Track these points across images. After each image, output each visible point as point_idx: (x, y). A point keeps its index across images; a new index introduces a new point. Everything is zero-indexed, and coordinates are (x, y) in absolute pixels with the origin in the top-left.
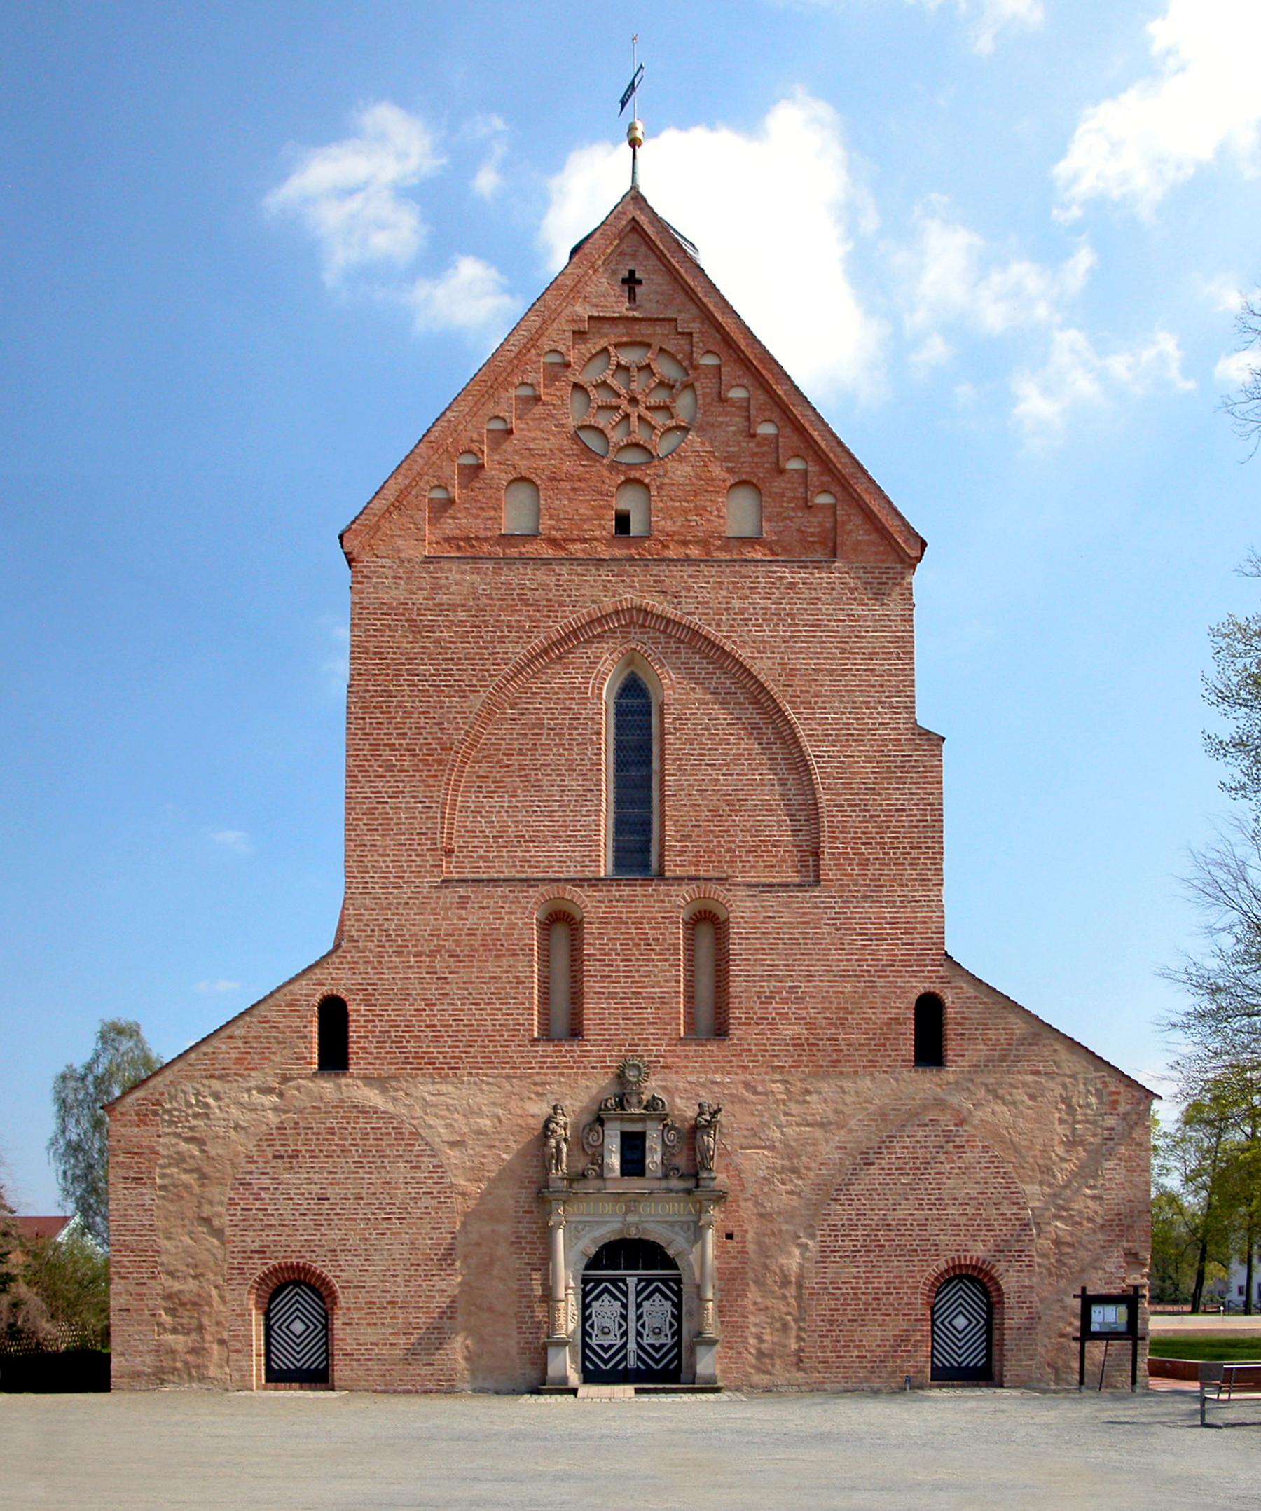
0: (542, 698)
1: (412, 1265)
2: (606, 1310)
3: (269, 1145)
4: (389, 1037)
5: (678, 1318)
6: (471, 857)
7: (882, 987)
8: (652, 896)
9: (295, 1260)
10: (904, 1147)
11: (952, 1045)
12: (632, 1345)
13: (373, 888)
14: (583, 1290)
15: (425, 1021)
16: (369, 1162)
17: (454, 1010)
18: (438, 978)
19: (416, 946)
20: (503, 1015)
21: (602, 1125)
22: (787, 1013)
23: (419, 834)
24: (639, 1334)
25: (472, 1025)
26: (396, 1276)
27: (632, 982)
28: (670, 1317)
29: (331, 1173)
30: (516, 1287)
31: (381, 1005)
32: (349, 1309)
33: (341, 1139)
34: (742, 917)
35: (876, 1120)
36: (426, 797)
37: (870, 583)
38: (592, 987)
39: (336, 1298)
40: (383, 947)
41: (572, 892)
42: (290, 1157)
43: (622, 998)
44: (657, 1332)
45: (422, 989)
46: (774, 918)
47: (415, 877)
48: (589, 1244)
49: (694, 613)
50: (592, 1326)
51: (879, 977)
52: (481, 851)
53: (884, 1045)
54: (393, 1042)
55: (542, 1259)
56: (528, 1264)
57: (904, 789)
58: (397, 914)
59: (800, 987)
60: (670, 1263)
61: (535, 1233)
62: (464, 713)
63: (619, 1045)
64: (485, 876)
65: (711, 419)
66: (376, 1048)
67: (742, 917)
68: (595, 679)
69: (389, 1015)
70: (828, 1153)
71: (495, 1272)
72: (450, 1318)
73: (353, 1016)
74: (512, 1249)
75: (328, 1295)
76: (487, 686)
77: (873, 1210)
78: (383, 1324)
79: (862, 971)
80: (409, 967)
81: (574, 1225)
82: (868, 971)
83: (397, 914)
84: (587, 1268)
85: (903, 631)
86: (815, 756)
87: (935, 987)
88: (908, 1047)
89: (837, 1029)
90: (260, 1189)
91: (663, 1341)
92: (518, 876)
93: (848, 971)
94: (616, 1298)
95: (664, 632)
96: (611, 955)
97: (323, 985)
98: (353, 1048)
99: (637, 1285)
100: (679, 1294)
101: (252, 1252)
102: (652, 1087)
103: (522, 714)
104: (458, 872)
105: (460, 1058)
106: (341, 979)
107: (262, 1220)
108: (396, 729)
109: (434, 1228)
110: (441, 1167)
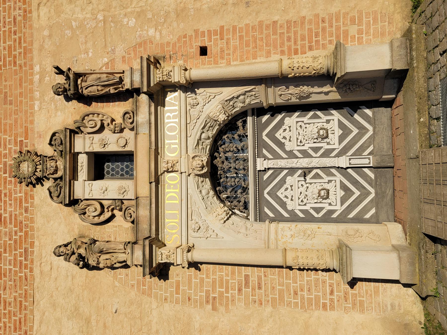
63: (5, 183)
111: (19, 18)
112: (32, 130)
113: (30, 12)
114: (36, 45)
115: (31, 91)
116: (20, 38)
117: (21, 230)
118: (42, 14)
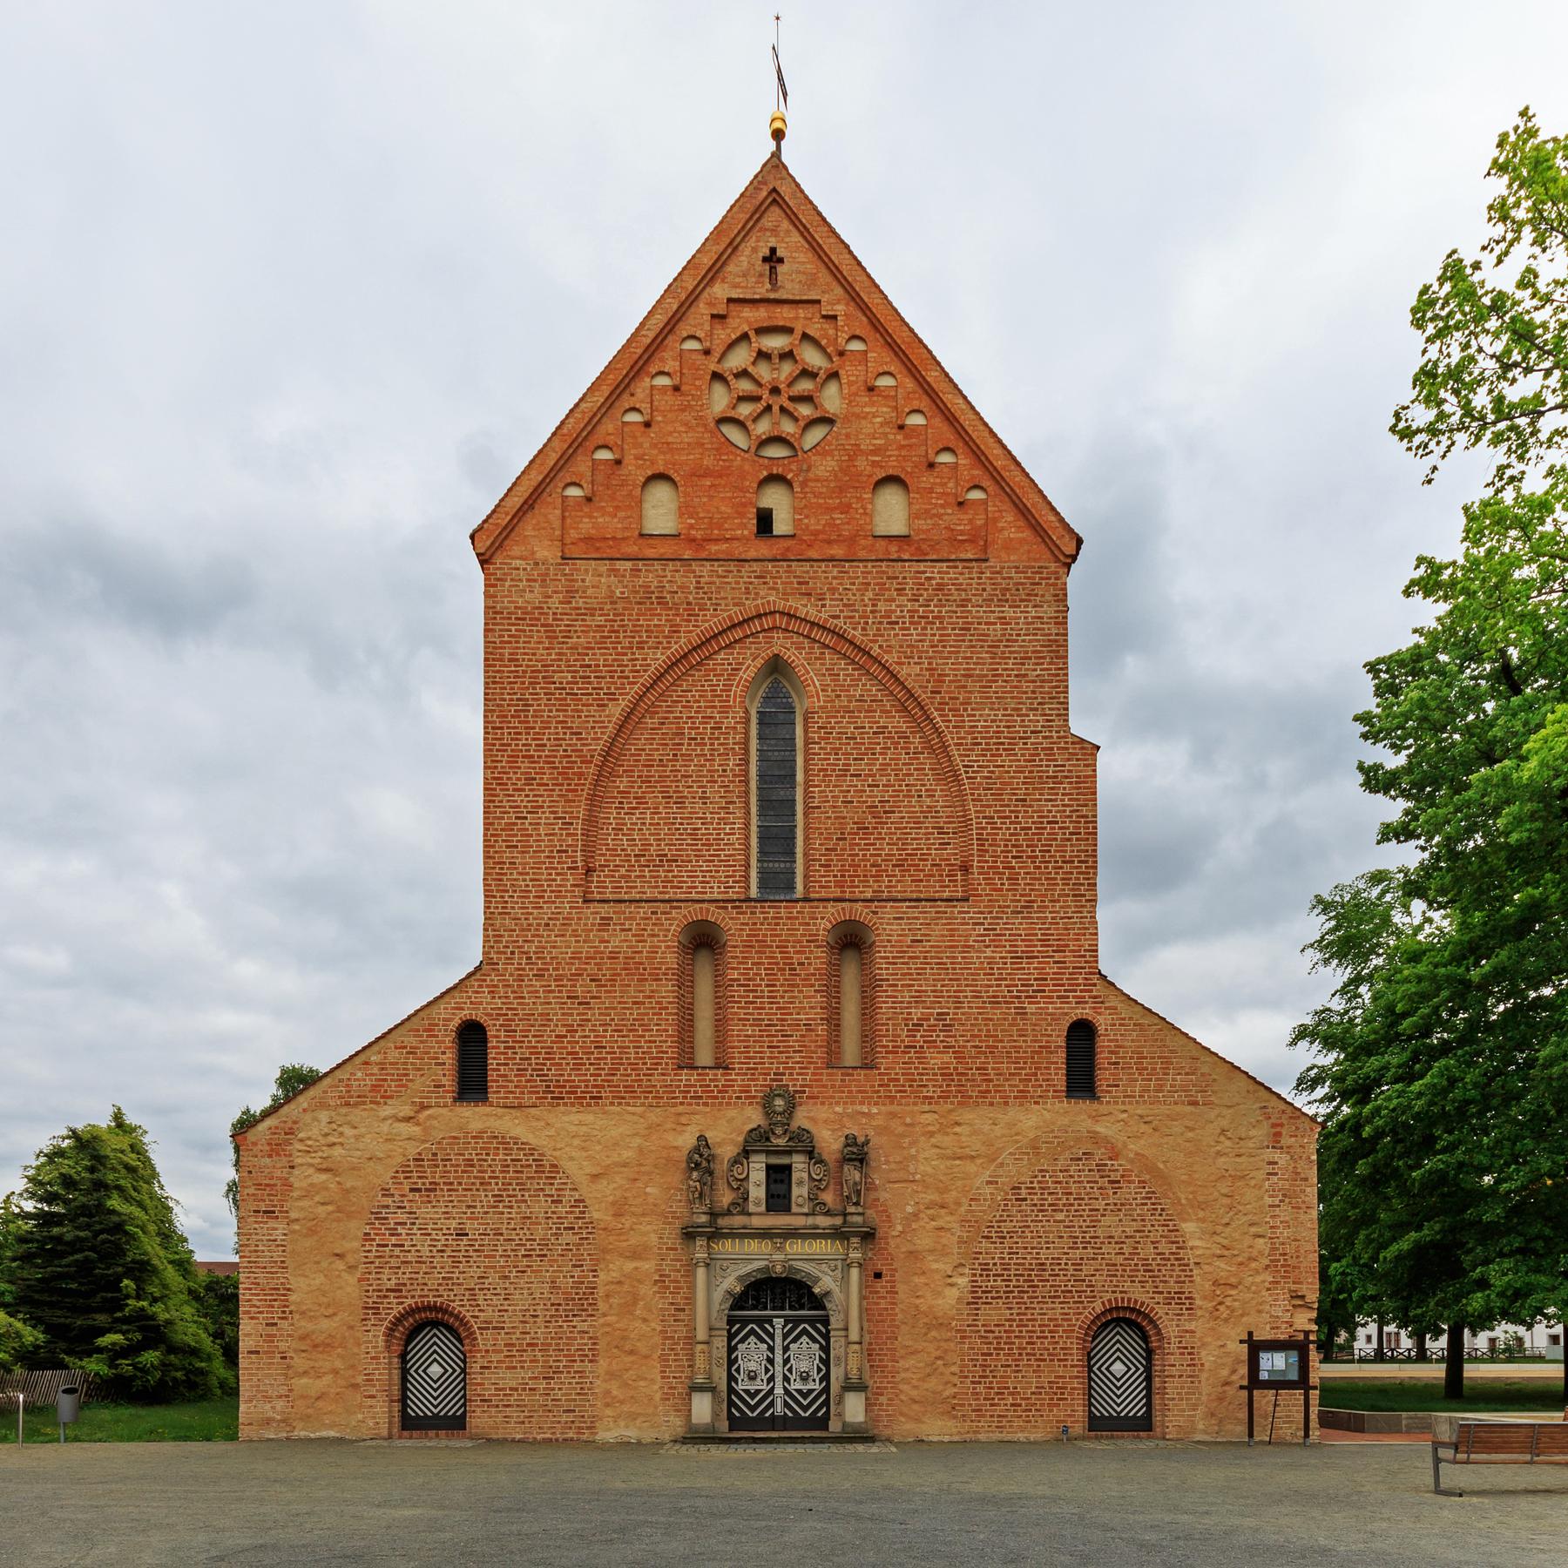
0: (683, 707)
1: (552, 1305)
2: (752, 1355)
3: (406, 1178)
4: (530, 1064)
5: (826, 1362)
6: (613, 876)
7: (1032, 1014)
8: (797, 918)
9: (432, 1300)
10: (1056, 1182)
11: (1103, 1077)
12: (779, 1391)
13: (513, 908)
14: (729, 1331)
15: (566, 1048)
16: (509, 1196)
17: (595, 1037)
18: (579, 1004)
19: (557, 969)
20: (646, 1042)
21: (747, 1158)
22: (935, 1041)
23: (558, 851)
24: (786, 1379)
25: (615, 1053)
26: (537, 1316)
27: (778, 1008)
28: (817, 1361)
29: (469, 1207)
30: (659, 1328)
31: (521, 1031)
32: (487, 1351)
33: (479, 1172)
34: (889, 941)
35: (1028, 1154)
36: (566, 812)
37: (1022, 584)
38: (736, 1013)
39: (476, 1339)
40: (524, 969)
41: (714, 914)
42: (427, 1190)
43: (767, 1025)
44: (805, 1378)
45: (563, 1014)
46: (921, 941)
47: (556, 897)
48: (730, 1282)
49: (839, 617)
50: (738, 1370)
51: (1029, 1003)
52: (623, 871)
53: (1036, 1074)
54: (533, 1070)
55: (686, 1298)
56: (672, 1304)
57: (1056, 800)
58: (538, 936)
59: (948, 1014)
60: (817, 1302)
61: (679, 1271)
62: (603, 722)
64: (627, 897)
65: (857, 410)
66: (516, 1076)
67: (889, 941)
68: (737, 686)
69: (530, 1042)
70: (978, 1188)
71: (638, 1312)
72: (591, 1361)
73: (492, 1043)
74: (655, 1289)
75: (467, 1337)
76: (628, 694)
77: (1026, 1248)
78: (522, 1367)
79: (1012, 997)
80: (550, 992)
81: (719, 1263)
82: (1019, 997)
83: (538, 936)
84: (732, 1309)
85: (1057, 634)
86: (964, 766)
87: (1085, 1012)
88: (1060, 1079)
89: (987, 1058)
90: (396, 1224)
91: (811, 1386)
92: (660, 897)
93: (998, 997)
94: (763, 1341)
95: (808, 637)
96: (755, 980)
97: (462, 1009)
98: (492, 1075)
99: (784, 1327)
100: (827, 1337)
101: (388, 1290)
102: (801, 1119)
103: (663, 723)
104: (599, 893)
105: (603, 1087)
106: (481, 1003)
107: (398, 1257)
108: (534, 739)
109: (574, 1266)
110: (583, 1201)
111: (925, 1090)
112: (816, 1104)
113: (930, 1103)
114: (895, 1108)
115: (853, 1103)
116: (905, 1091)
117: (719, 1092)
118: (927, 1115)
